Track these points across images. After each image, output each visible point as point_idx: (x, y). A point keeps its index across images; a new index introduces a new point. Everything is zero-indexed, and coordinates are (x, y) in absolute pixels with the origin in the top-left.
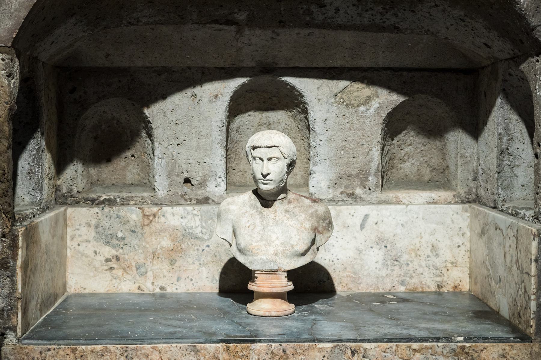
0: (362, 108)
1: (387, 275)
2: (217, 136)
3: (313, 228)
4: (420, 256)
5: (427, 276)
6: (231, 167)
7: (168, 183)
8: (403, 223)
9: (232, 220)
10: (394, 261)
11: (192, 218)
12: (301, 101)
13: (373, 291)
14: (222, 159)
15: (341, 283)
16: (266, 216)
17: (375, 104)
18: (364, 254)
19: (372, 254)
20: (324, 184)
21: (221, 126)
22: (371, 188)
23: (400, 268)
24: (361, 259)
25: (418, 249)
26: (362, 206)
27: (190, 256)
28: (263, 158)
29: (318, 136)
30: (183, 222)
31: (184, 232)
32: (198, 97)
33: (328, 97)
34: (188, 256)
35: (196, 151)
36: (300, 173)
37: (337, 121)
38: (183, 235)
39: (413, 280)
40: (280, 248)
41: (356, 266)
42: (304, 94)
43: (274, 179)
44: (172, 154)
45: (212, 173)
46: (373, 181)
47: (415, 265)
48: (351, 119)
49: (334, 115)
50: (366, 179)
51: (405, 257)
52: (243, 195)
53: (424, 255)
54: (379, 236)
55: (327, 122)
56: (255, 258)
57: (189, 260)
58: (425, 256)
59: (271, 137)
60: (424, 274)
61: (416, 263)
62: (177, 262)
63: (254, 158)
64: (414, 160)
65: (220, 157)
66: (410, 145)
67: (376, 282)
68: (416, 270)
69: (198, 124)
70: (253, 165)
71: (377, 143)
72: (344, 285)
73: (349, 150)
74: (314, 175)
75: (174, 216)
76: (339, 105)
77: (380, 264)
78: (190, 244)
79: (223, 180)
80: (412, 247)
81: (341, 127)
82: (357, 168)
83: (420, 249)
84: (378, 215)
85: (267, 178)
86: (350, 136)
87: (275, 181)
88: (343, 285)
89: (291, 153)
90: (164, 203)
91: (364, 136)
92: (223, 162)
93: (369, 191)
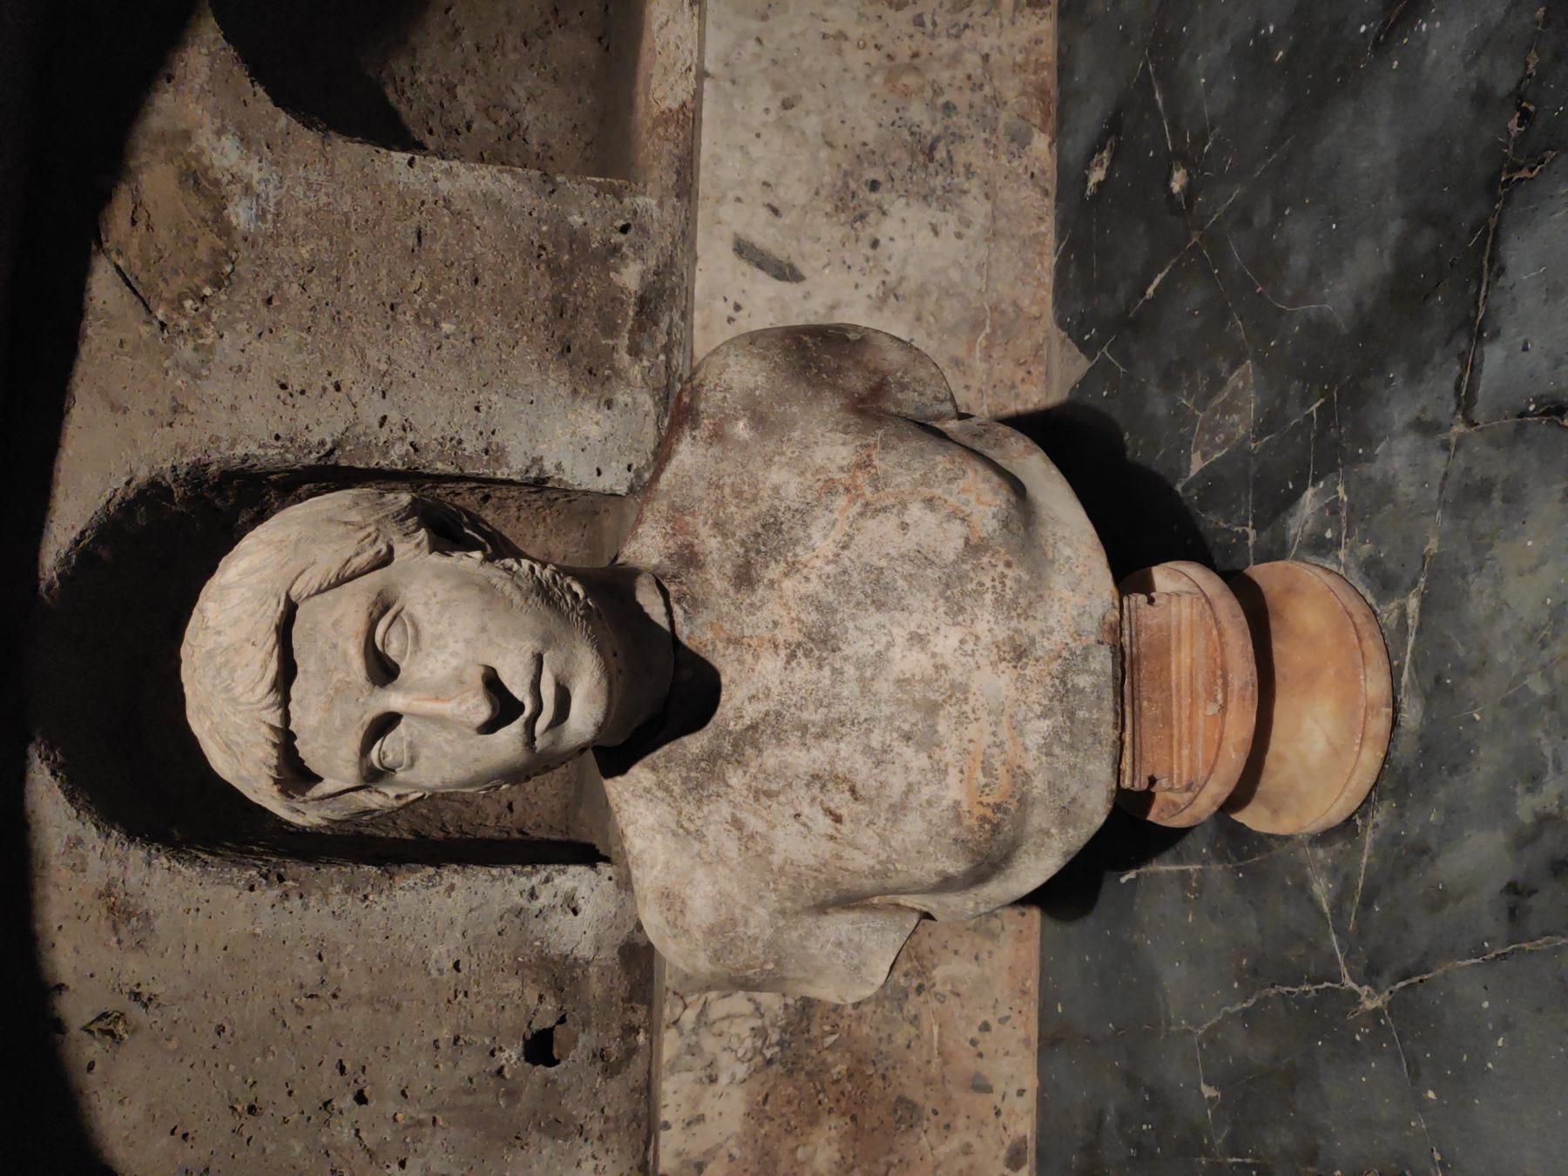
0: (240, 214)
1: (987, 196)
2: (326, 910)
3: (853, 420)
4: (915, 55)
5: (996, 42)
6: (498, 818)
7: (546, 1141)
8: (779, 104)
9: (783, 912)
10: (931, 160)
11: (716, 1029)
12: (185, 501)
13: (1051, 261)
14: (446, 883)
15: (1013, 387)
16: (772, 705)
17: (225, 155)
18: (902, 279)
19: (901, 245)
20: (591, 422)
21: (276, 892)
22: (620, 223)
23: (962, 139)
24: (922, 292)
25: (890, 57)
26: (700, 265)
27: (884, 1035)
28: (368, 718)
29: (360, 429)
30: (733, 1076)
31: (776, 1068)
32: (112, 1004)
33: (167, 364)
34: (883, 1048)
35: (398, 1008)
36: (540, 539)
37: (291, 336)
38: (790, 1073)
39: (1011, 95)
40: (981, 627)
41: (949, 317)
42: (143, 475)
43: (529, 646)
44: (407, 1127)
45: (508, 931)
46: (587, 212)
47: (953, 77)
48: (287, 271)
49: (263, 347)
50: (577, 239)
51: (917, 112)
52: (629, 831)
53: (911, 37)
54: (829, 208)
55: (295, 384)
56: (1039, 785)
57: (900, 1040)
58: (918, 36)
59: (210, 655)
60: (986, 50)
61: (945, 76)
62: (909, 1094)
63: (374, 776)
64: (516, 87)
65: (436, 897)
66: (451, 90)
67: (1015, 243)
68: (969, 77)
69: (259, 999)
70: (427, 783)
71: (417, 169)
72: (1021, 373)
73: (440, 298)
74: (549, 466)
75: (700, 1119)
76: (214, 317)
77: (939, 217)
78: (830, 1040)
79: (547, 880)
80: (878, 79)
81: (325, 320)
82: (525, 274)
83: (890, 48)
84: (738, 200)
85: (519, 689)
86: (374, 285)
87: (548, 640)
88: (1023, 380)
89: (355, 516)
90: (639, 1157)
91: (377, 223)
92: (457, 880)
93: (631, 233)
